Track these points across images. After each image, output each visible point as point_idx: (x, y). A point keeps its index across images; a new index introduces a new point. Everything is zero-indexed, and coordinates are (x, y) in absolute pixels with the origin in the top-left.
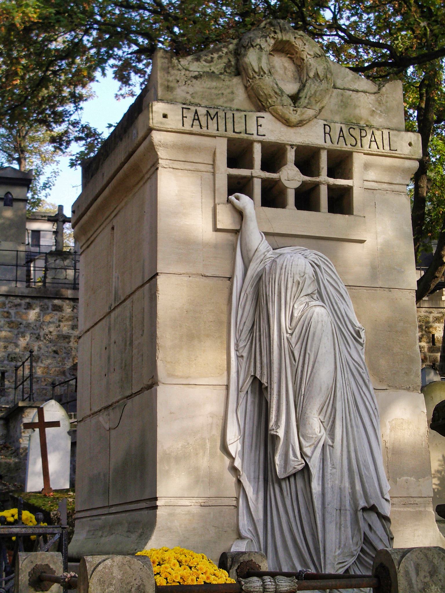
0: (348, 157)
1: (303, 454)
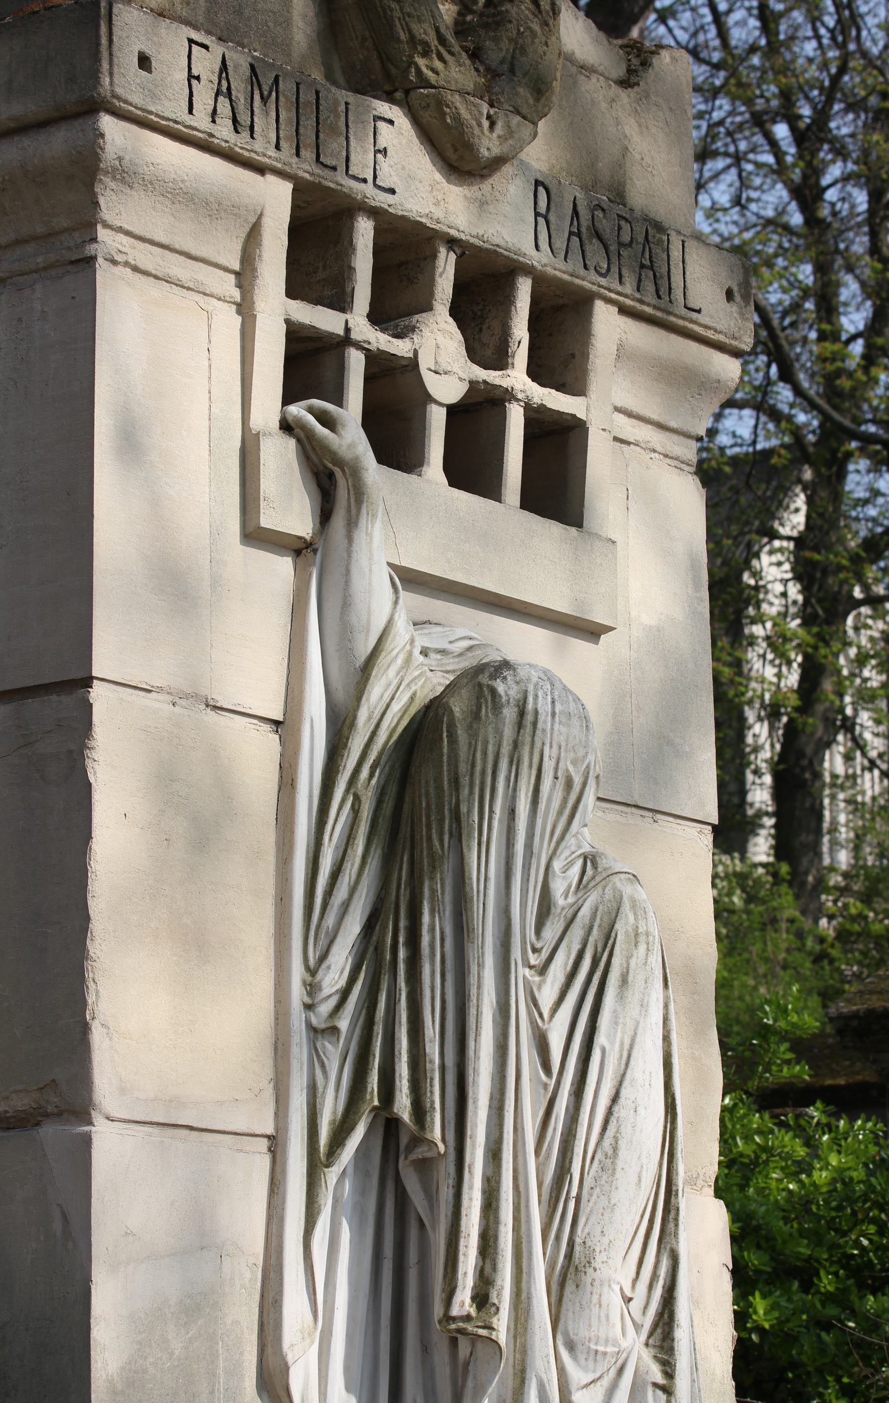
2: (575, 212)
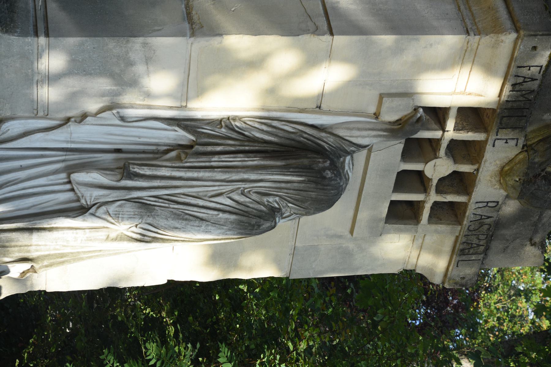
0: (456, 216)
2: (489, 217)
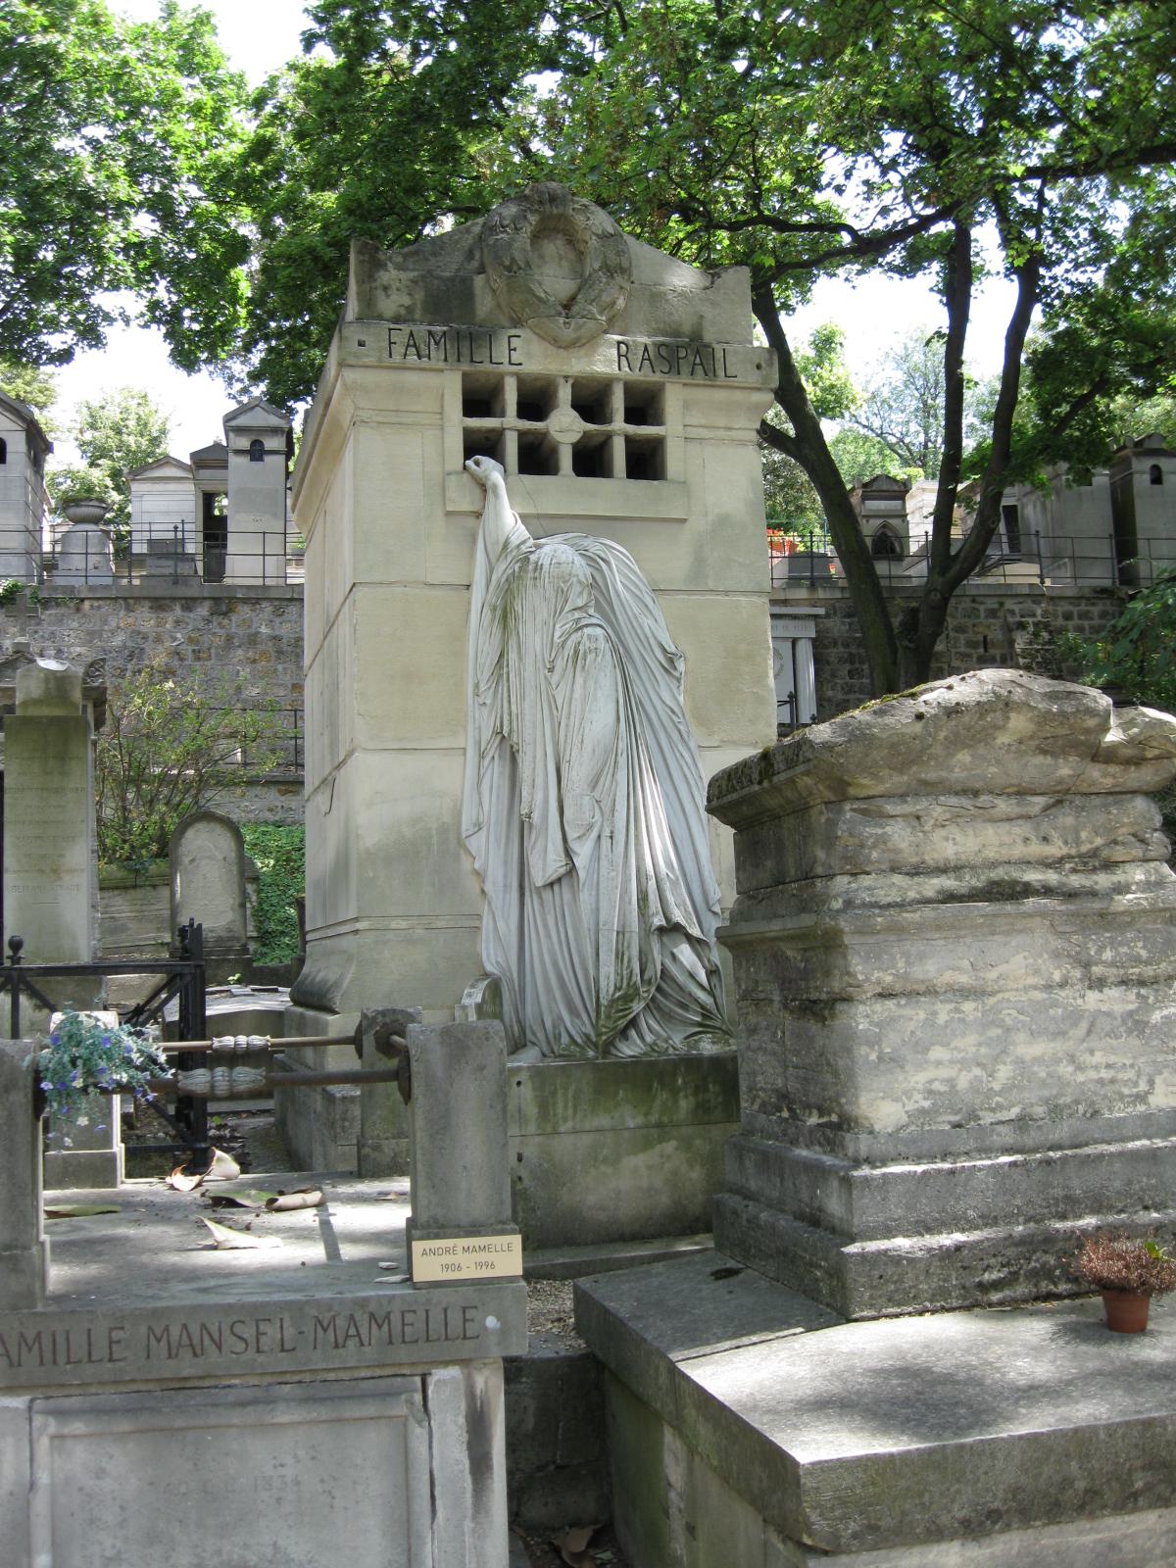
1: (568, 853)
